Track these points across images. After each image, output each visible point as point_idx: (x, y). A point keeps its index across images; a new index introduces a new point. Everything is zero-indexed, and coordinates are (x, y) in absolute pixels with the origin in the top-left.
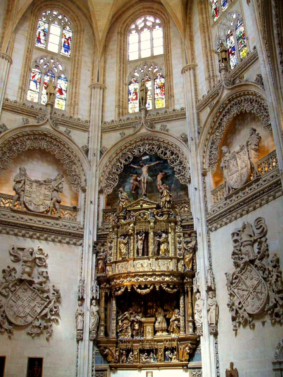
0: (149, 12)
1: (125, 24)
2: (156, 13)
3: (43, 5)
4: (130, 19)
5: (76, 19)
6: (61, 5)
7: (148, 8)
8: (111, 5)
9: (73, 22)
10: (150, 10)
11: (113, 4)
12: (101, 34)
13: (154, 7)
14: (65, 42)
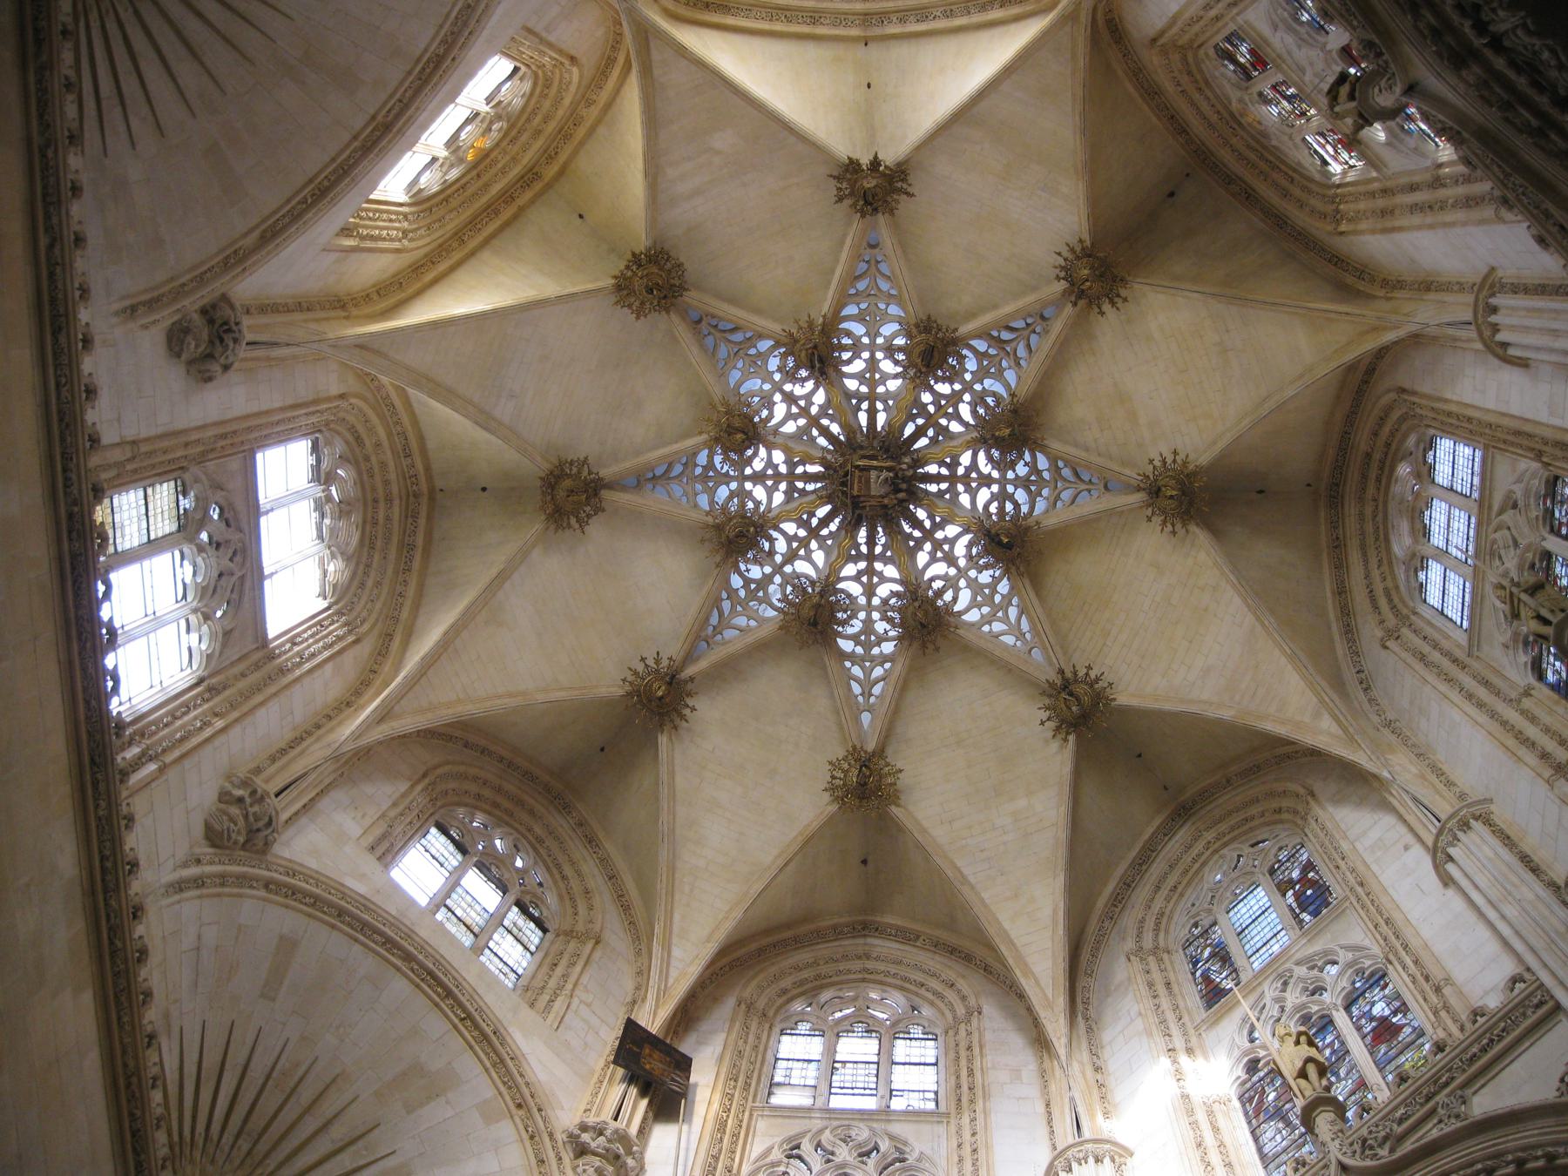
0: (1378, 480)
1: (1383, 602)
2: (1388, 445)
3: (1156, 907)
4: (1376, 573)
5: (1274, 805)
6: (1209, 836)
7: (1364, 477)
8: (1259, 628)
9: (1281, 822)
10: (1373, 474)
11: (1258, 618)
12: (1327, 723)
13: (1364, 446)
14: (1297, 896)
